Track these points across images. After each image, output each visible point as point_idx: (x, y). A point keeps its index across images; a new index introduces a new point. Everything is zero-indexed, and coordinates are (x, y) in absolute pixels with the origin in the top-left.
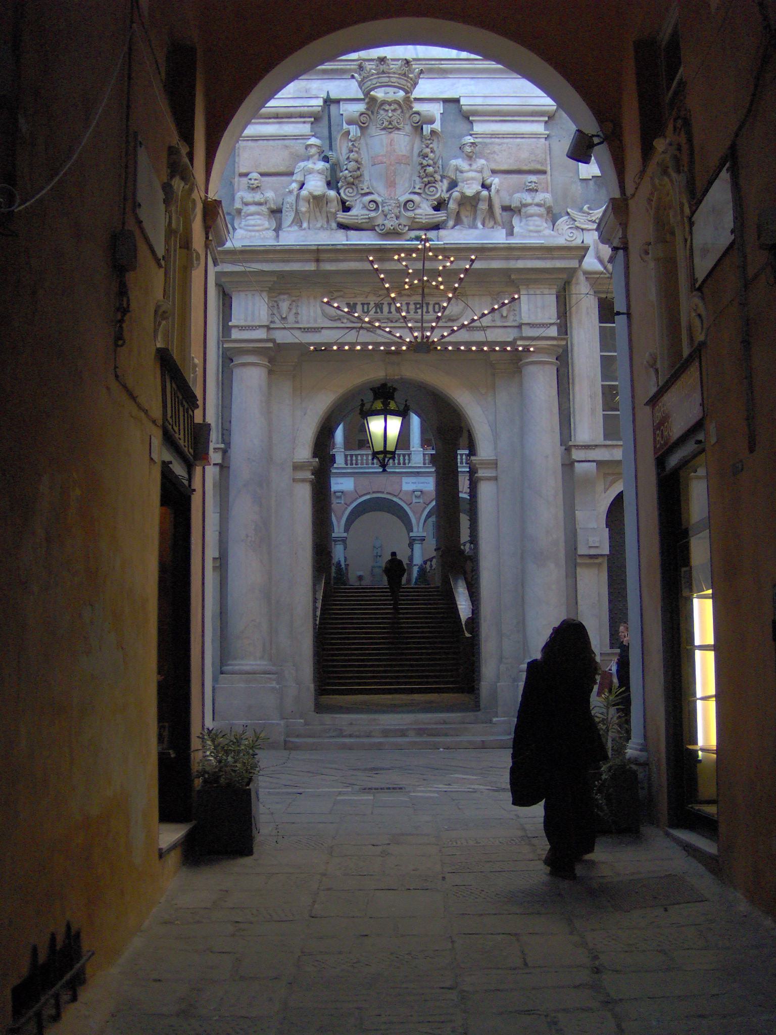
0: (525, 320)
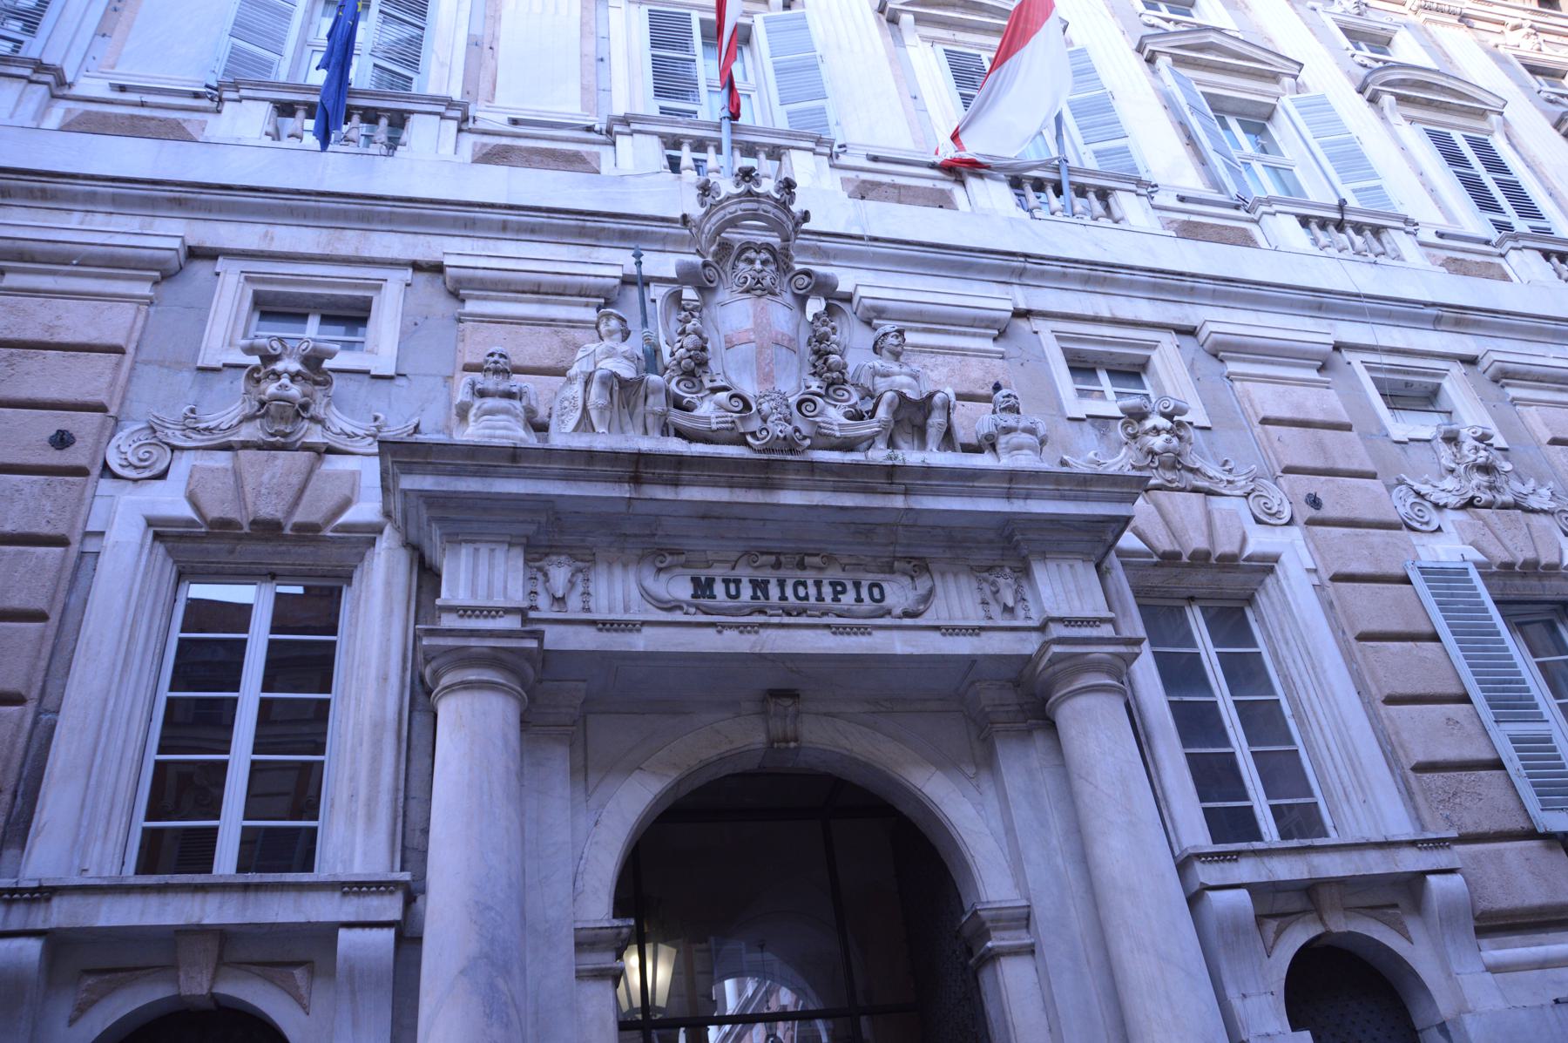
0: (1055, 614)
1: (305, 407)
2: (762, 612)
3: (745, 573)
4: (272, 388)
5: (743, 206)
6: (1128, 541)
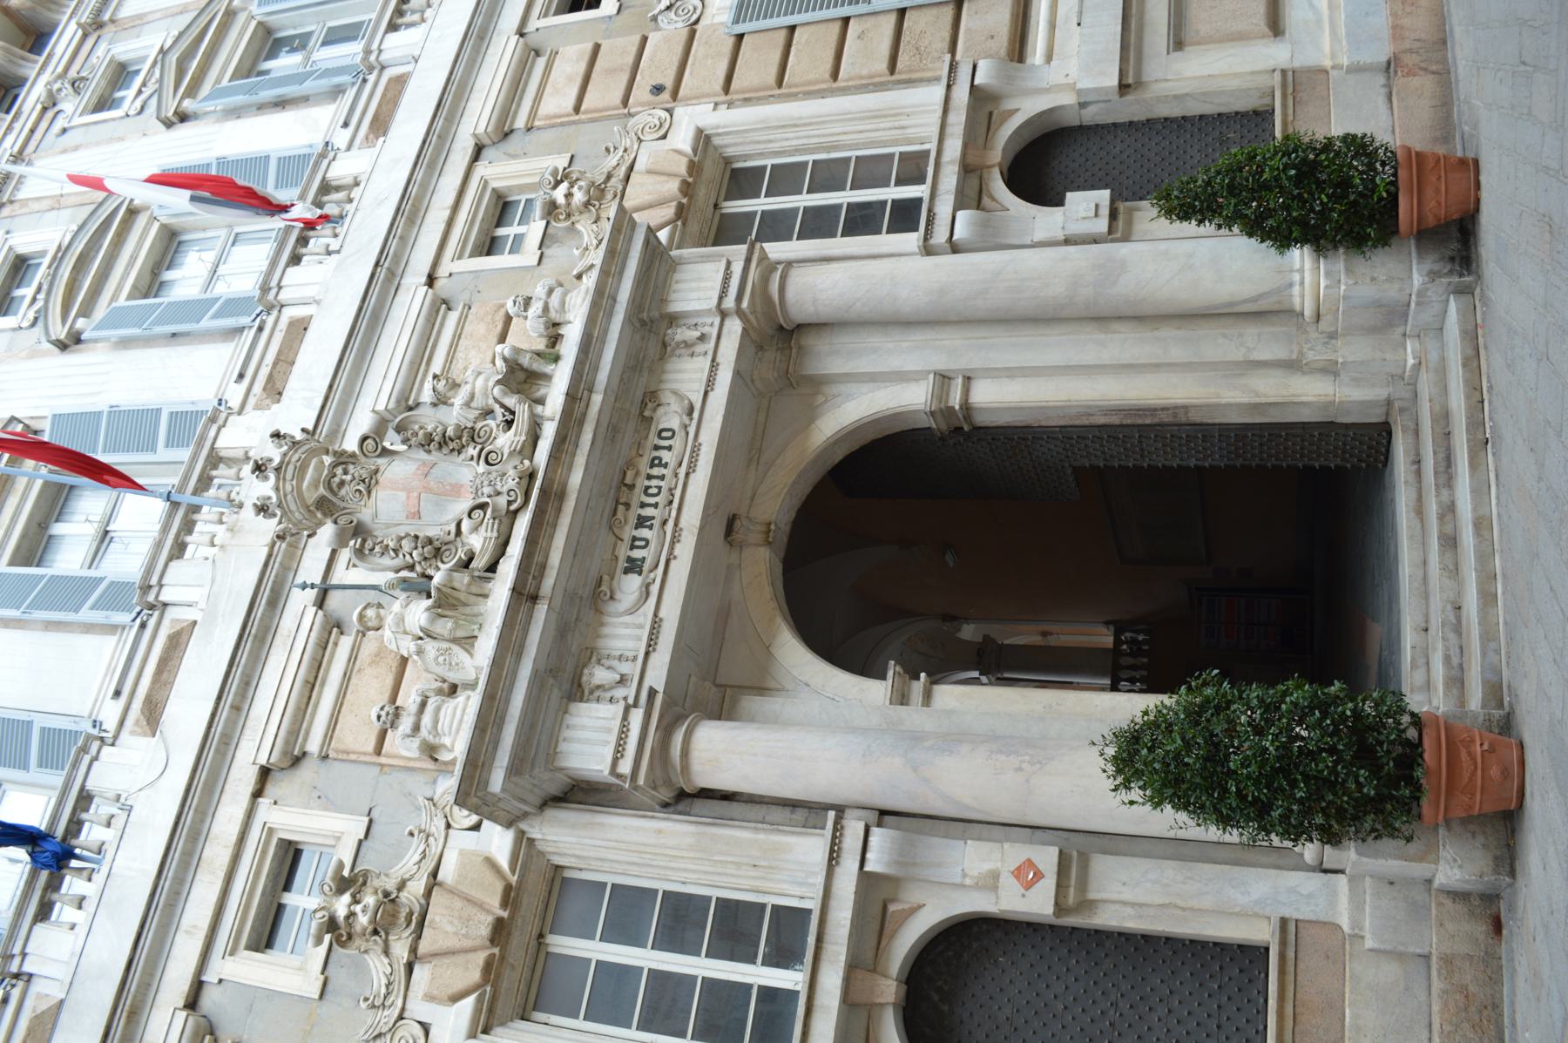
0: (715, 301)
1: (386, 894)
2: (665, 522)
3: (628, 532)
4: (363, 920)
5: (289, 476)
6: (663, 235)
